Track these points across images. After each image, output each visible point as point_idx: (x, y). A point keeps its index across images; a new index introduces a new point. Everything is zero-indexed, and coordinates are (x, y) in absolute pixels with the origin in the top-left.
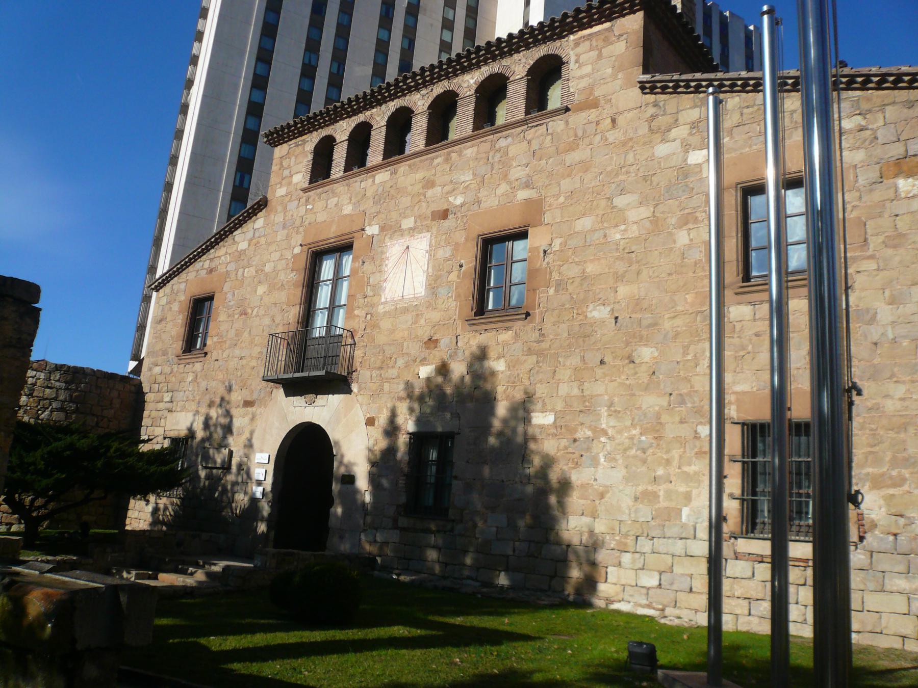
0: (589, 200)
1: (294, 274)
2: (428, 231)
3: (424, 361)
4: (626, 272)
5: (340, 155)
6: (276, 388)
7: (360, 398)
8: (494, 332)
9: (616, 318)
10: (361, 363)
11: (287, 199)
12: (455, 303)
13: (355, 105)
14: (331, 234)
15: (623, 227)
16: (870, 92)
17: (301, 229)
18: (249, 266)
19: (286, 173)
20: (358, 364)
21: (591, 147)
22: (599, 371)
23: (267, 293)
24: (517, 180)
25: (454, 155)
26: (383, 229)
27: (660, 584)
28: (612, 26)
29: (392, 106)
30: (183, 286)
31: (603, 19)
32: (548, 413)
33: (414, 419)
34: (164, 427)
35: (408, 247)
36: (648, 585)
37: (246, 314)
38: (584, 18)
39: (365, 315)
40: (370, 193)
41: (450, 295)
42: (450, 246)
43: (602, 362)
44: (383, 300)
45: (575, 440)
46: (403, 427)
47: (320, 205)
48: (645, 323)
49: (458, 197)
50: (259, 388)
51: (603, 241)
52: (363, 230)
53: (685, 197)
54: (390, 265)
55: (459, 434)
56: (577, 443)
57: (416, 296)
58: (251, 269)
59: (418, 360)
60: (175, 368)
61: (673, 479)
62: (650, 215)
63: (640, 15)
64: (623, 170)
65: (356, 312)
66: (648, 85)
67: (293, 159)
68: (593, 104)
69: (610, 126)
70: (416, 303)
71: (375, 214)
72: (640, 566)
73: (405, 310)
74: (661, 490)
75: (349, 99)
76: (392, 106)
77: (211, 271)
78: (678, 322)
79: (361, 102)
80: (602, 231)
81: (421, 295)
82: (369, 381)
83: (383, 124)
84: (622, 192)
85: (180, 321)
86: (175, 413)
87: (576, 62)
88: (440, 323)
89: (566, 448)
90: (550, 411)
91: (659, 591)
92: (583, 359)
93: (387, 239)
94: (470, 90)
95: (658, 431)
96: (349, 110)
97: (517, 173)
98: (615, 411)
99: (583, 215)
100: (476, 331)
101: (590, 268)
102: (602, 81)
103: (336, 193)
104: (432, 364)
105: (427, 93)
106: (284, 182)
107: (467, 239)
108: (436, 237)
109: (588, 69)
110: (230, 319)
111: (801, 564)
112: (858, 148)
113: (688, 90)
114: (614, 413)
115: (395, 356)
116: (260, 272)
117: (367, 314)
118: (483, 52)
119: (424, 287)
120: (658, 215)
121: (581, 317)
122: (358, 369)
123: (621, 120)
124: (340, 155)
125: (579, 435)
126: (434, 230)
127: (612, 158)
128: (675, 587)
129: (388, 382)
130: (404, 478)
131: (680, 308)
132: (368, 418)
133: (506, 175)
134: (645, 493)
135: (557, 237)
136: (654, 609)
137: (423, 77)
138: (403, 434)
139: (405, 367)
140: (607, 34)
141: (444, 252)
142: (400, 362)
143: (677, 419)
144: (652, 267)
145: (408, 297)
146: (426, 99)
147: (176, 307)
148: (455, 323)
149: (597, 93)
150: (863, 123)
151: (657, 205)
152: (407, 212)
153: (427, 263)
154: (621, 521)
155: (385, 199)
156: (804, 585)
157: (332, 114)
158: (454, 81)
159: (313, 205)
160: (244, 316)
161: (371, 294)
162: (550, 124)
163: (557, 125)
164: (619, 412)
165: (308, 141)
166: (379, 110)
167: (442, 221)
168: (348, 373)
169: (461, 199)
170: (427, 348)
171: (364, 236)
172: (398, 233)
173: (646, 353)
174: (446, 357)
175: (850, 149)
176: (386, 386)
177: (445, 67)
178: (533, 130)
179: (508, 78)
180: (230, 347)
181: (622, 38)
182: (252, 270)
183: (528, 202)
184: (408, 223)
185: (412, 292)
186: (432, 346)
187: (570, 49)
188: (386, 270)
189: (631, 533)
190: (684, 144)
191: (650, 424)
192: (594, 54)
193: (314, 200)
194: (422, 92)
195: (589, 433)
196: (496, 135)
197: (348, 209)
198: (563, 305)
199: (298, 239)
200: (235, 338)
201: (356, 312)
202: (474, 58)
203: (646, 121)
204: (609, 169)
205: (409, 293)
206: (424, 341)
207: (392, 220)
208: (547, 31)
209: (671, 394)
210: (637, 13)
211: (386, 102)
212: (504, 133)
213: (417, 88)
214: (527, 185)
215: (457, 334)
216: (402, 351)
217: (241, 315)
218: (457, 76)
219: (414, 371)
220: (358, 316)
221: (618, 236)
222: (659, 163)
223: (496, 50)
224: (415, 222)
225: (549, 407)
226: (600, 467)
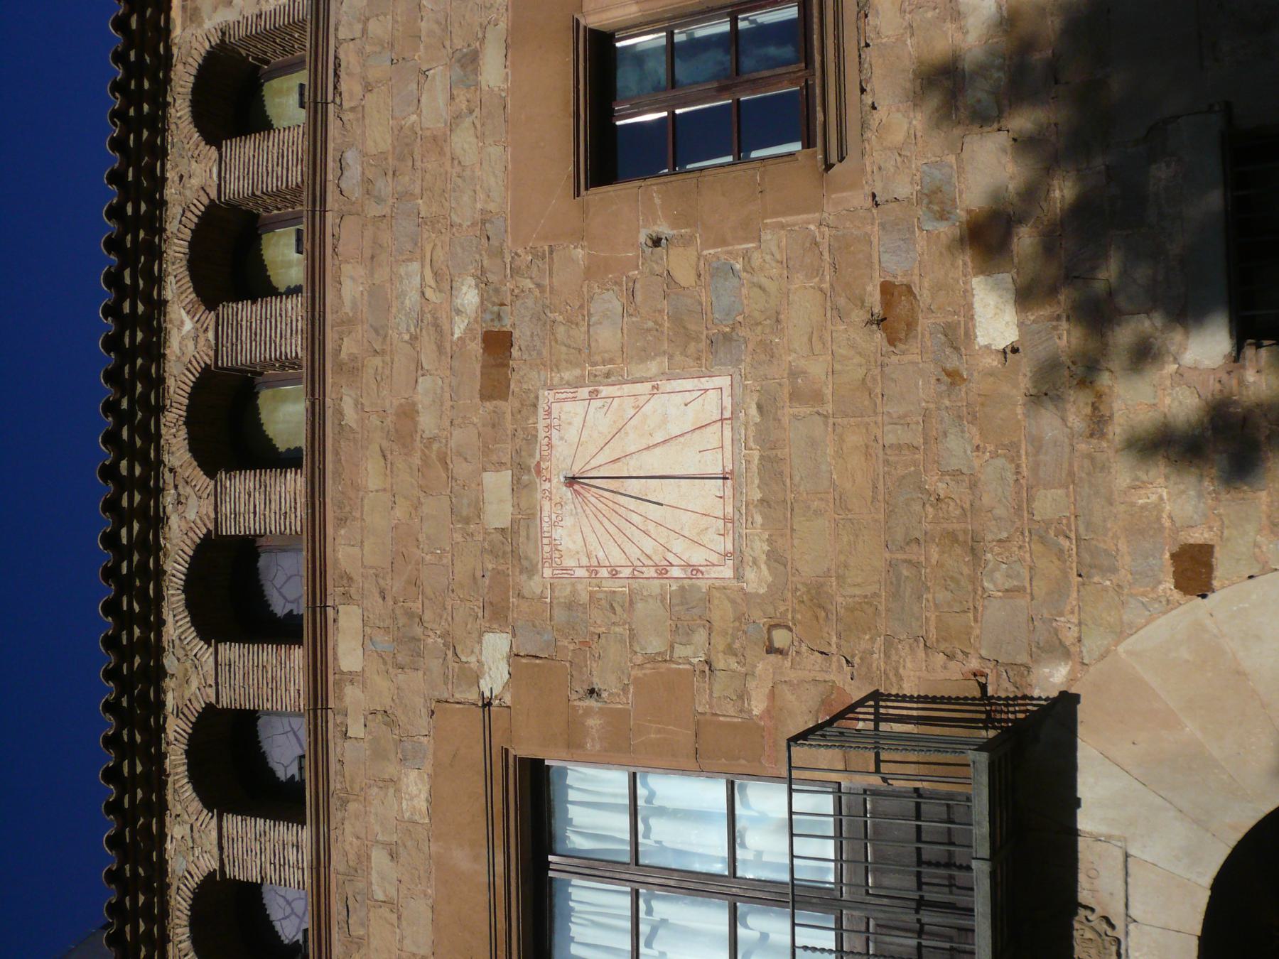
2: (535, 406)
7: (1093, 645)
8: (868, 54)
10: (950, 657)
12: (767, 236)
20: (955, 671)
26: (498, 614)
33: (1177, 336)
39: (772, 657)
41: (738, 267)
46: (1212, 388)
52: (487, 704)
54: (617, 557)
57: (727, 414)
59: (953, 362)
70: (753, 411)
71: (450, 653)
73: (772, 468)
79: (131, 737)
81: (727, 391)
82: (1022, 602)
88: (826, 286)
93: (534, 586)
100: (864, 125)
104: (968, 293)
105: (176, 487)
107: (580, 236)
108: (556, 367)
117: (771, 650)
118: (127, 273)
119: (706, 383)
122: (974, 664)
129: (1030, 499)
137: (124, 484)
138: (1241, 382)
139: (974, 419)
145: (728, 454)
146: (188, 490)
148: (831, 220)
152: (464, 513)
153: (627, 389)
155: (410, 615)
157: (134, 871)
158: (172, 390)
161: (700, 636)
167: (515, 352)
168: (988, 723)
169: (464, 289)
170: (911, 325)
171: (508, 699)
174: (946, 230)
176: (1049, 503)
177: (125, 404)
178: (343, 87)
179: (212, 201)
184: (497, 483)
186: (902, 308)
187: (199, 31)
188: (626, 572)
194: (169, 509)
201: (758, 707)
202: (134, 307)
206: (887, 348)
207: (479, 574)
211: (159, 651)
212: (330, 177)
214: (470, 61)
218: (161, 380)
219: (991, 373)
220: (772, 695)
223: (136, 236)
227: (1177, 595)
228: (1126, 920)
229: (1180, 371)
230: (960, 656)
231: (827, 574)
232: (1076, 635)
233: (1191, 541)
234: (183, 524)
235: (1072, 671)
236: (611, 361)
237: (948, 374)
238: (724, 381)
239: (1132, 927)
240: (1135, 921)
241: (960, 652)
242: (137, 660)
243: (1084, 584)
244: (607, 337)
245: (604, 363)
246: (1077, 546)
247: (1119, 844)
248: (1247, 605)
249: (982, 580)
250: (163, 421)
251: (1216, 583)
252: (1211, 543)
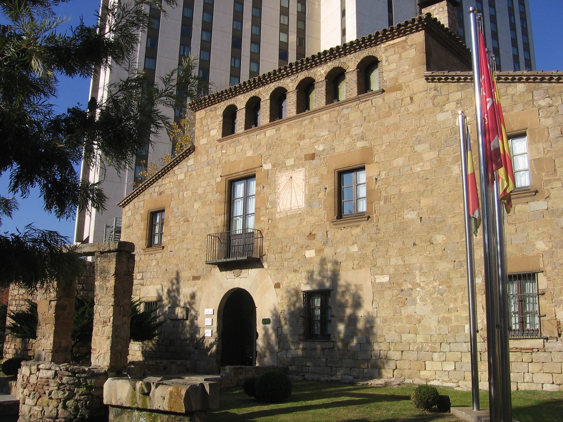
0: (401, 147)
1: (218, 195)
2: (303, 167)
3: (308, 247)
4: (425, 190)
5: (241, 118)
6: (214, 267)
7: (269, 271)
8: (349, 228)
9: (421, 218)
10: (268, 250)
11: (208, 146)
12: (324, 211)
13: (248, 86)
14: (240, 169)
15: (421, 164)
16: (553, 84)
17: (220, 166)
18: (187, 190)
19: (206, 129)
20: (266, 251)
21: (400, 114)
22: (413, 250)
23: (201, 207)
24: (356, 135)
25: (315, 119)
26: (274, 166)
27: (455, 369)
28: (406, 39)
29: (272, 86)
30: (142, 204)
31: (401, 35)
32: (385, 275)
34: (140, 295)
35: (291, 178)
36: (449, 370)
37: (188, 221)
38: (389, 34)
40: (263, 143)
41: (320, 206)
42: (318, 176)
43: (414, 244)
44: (278, 210)
45: (402, 290)
47: (231, 150)
48: (437, 220)
49: (320, 146)
51: (410, 172)
52: (261, 166)
53: (456, 145)
54: (281, 189)
55: (333, 290)
56: (404, 292)
57: (299, 207)
58: (188, 191)
59: (304, 247)
60: (143, 257)
61: (459, 309)
62: (436, 156)
63: (422, 33)
64: (419, 129)
65: (262, 218)
66: (430, 78)
67: (209, 120)
68: (397, 88)
69: (410, 102)
70: (300, 212)
71: (268, 156)
72: (444, 359)
73: (293, 216)
74: (453, 316)
75: (244, 83)
76: (272, 86)
77: (161, 194)
78: (456, 219)
80: (409, 166)
81: (302, 207)
83: (268, 98)
84: (420, 142)
85: (142, 227)
86: (146, 287)
87: (387, 61)
89: (397, 295)
90: (386, 274)
91: (455, 372)
92: (403, 243)
93: (277, 173)
94: (322, 77)
95: (449, 282)
96: (245, 89)
97: (356, 131)
98: (424, 272)
99: (397, 157)
101: (404, 189)
102: (403, 74)
103: (241, 143)
106: (204, 135)
107: (328, 172)
108: (309, 171)
109: (393, 66)
110: (177, 224)
111: (530, 351)
112: (549, 117)
113: (454, 81)
114: (423, 274)
115: (289, 245)
116: (194, 194)
117: (269, 220)
119: (304, 202)
120: (441, 156)
121: (400, 218)
122: (267, 254)
123: (415, 98)
124: (241, 118)
125: (404, 287)
126: (307, 166)
127: (412, 121)
128: (463, 369)
130: (302, 318)
131: (457, 211)
133: (349, 132)
134: (444, 318)
135: (383, 170)
136: (452, 382)
139: (296, 251)
140: (404, 44)
141: (315, 180)
142: (293, 249)
143: (459, 275)
144: (440, 188)
145: (294, 208)
146: (294, 82)
147: (138, 217)
148: (325, 224)
149: (400, 81)
150: (551, 102)
151: (440, 150)
152: (288, 155)
153: (304, 187)
154: (431, 335)
155: (274, 146)
156: (532, 362)
157: (233, 92)
159: (226, 150)
160: (186, 223)
161: (270, 207)
162: (373, 100)
163: (378, 100)
164: (426, 273)
165: (218, 108)
166: (264, 89)
167: (311, 161)
170: (309, 239)
171: (262, 170)
172: (284, 169)
173: (439, 238)
175: (544, 117)
176: (286, 264)
178: (363, 103)
180: (179, 243)
181: (412, 47)
182: (189, 193)
183: (364, 148)
185: (296, 205)
186: (312, 238)
188: (279, 191)
189: (437, 341)
190: (453, 114)
191: (444, 279)
192: (397, 56)
193: (226, 147)
194: (291, 78)
195: (410, 286)
196: (340, 107)
197: (250, 153)
198: (390, 211)
199: (219, 172)
200: (182, 237)
201: (262, 218)
203: (431, 99)
204: (411, 128)
205: (295, 206)
206: (307, 235)
207: (279, 160)
208: (367, 42)
209: (455, 261)
210: (421, 32)
212: (345, 105)
213: (288, 75)
214: (362, 138)
215: (327, 230)
216: (293, 242)
217: (185, 222)
219: (302, 253)
220: (263, 221)
221: (419, 169)
222: (440, 125)
224: (295, 161)
225: (385, 272)
226: (418, 305)
227: (274, 283)
231: (278, 228)
234: (288, 83)
236: (308, 182)
238: (304, 206)
242: (264, 81)
244: (312, 181)
245: (308, 181)
250: (306, 71)
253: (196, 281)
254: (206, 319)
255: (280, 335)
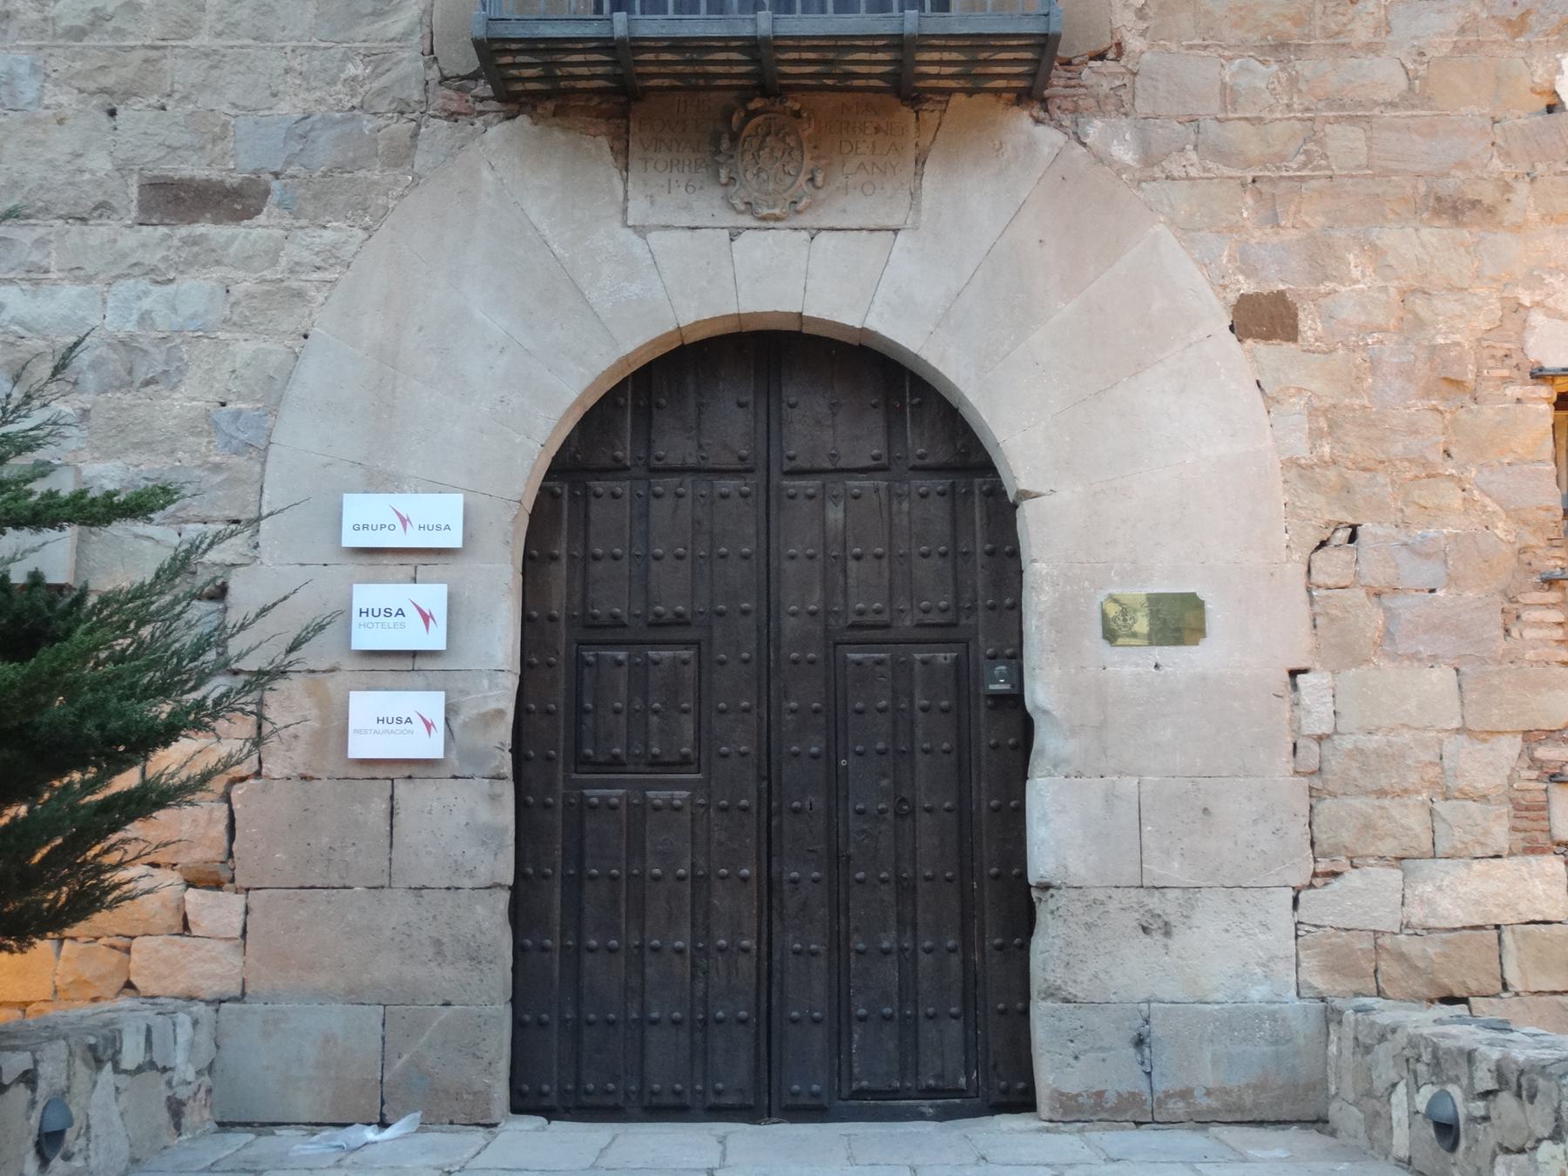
6: (453, 116)
50: (288, 108)
122: (1134, 43)
129: (1352, 119)
132: (1244, 298)
227: (1232, 297)
228: (813, 229)
229: (1521, 309)
230: (1143, 25)
232: (1176, 174)
233: (1301, 315)
235: (1127, 168)
237: (1523, 16)
239: (805, 235)
240: (812, 238)
241: (1146, 25)
243: (1243, 185)
246: (1291, 178)
247: (909, 221)
248: (1223, 378)
249: (1242, 56)
251: (1249, 342)
252: (1299, 338)
253: (201, 229)
254: (367, 595)
255: (1320, 739)
